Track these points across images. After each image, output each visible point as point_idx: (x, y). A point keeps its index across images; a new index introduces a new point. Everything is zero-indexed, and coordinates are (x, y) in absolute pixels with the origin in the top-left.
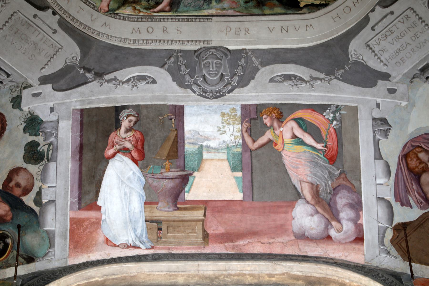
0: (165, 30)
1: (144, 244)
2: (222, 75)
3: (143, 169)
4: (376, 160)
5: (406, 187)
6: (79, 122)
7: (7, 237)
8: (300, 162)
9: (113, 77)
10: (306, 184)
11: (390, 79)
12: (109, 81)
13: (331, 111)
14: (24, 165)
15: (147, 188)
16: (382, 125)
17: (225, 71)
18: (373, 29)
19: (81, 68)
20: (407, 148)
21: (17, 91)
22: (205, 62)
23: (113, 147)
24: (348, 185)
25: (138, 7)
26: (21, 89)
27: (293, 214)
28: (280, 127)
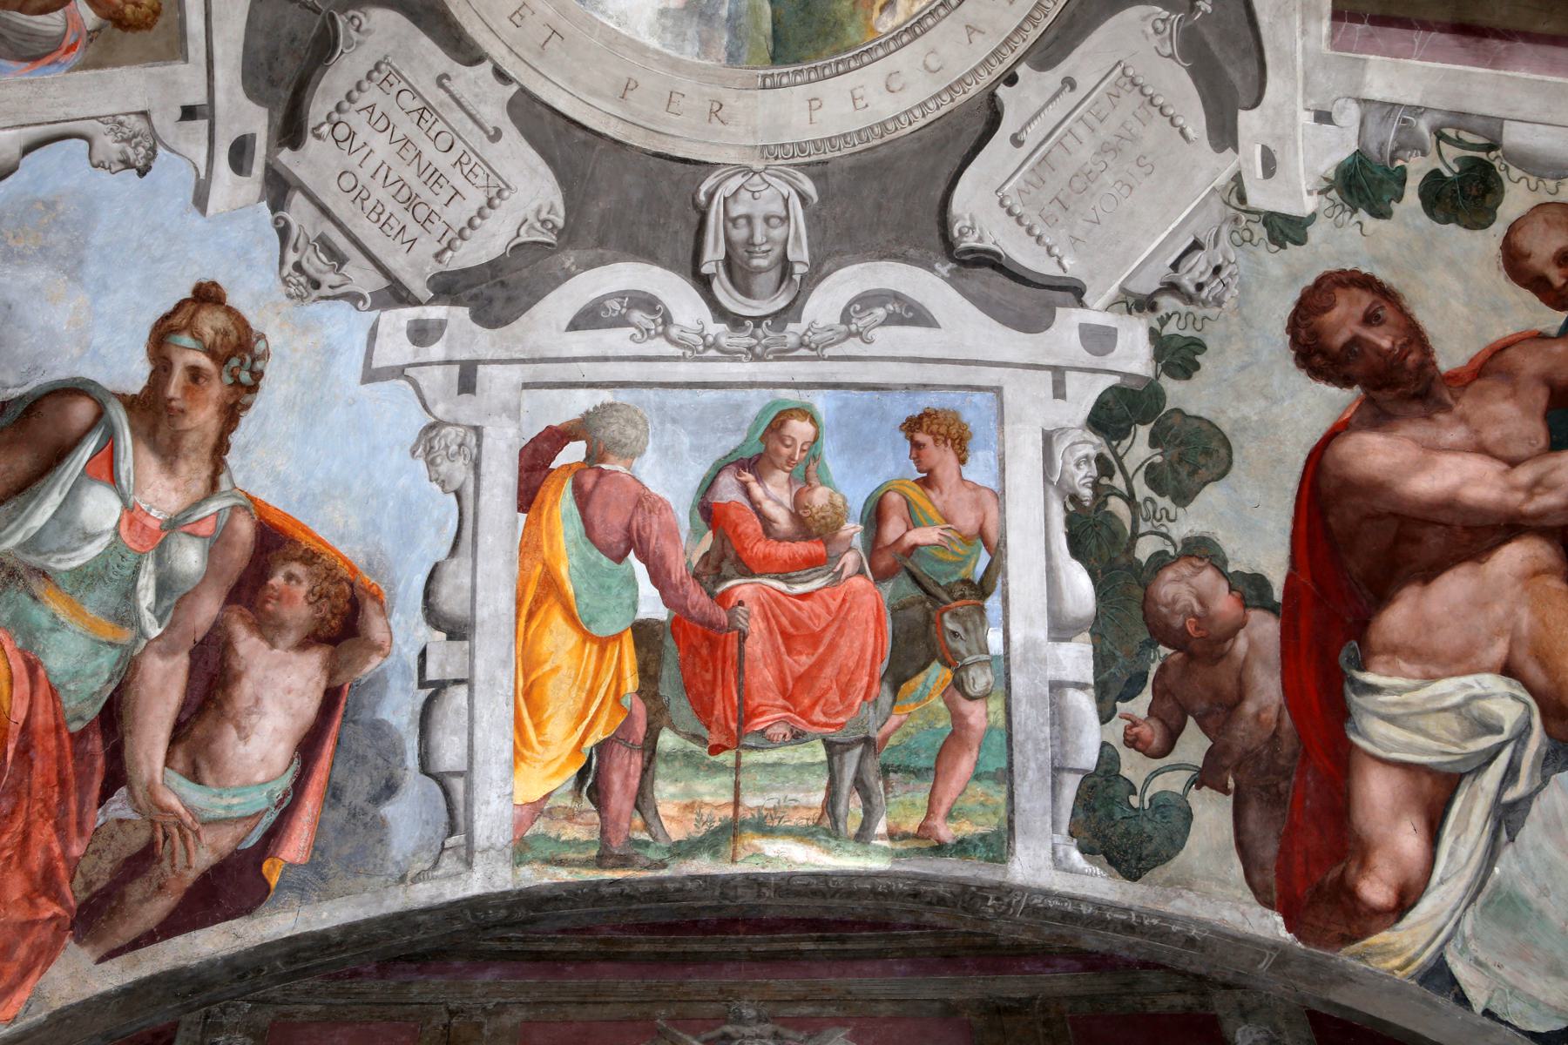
14: (1498, 229)
21: (1251, 226)
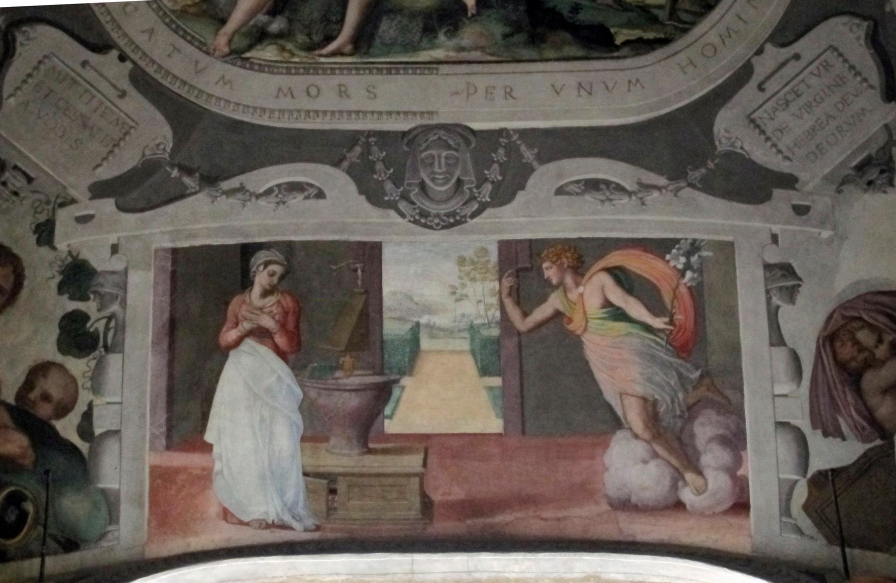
0: (343, 92)
1: (299, 519)
2: (459, 182)
3: (297, 368)
4: (773, 348)
5: (832, 398)
6: (168, 274)
7: (24, 498)
8: (620, 354)
9: (238, 185)
10: (633, 399)
11: (797, 186)
12: (229, 193)
13: (681, 252)
14: (59, 358)
15: (308, 409)
16: (784, 278)
17: (465, 172)
18: (761, 88)
19: (172, 166)
20: (833, 321)
21: (46, 211)
22: (424, 155)
23: (237, 324)
24: (717, 398)
25: (289, 46)
26: (54, 209)
27: (607, 459)
28: (577, 284)
